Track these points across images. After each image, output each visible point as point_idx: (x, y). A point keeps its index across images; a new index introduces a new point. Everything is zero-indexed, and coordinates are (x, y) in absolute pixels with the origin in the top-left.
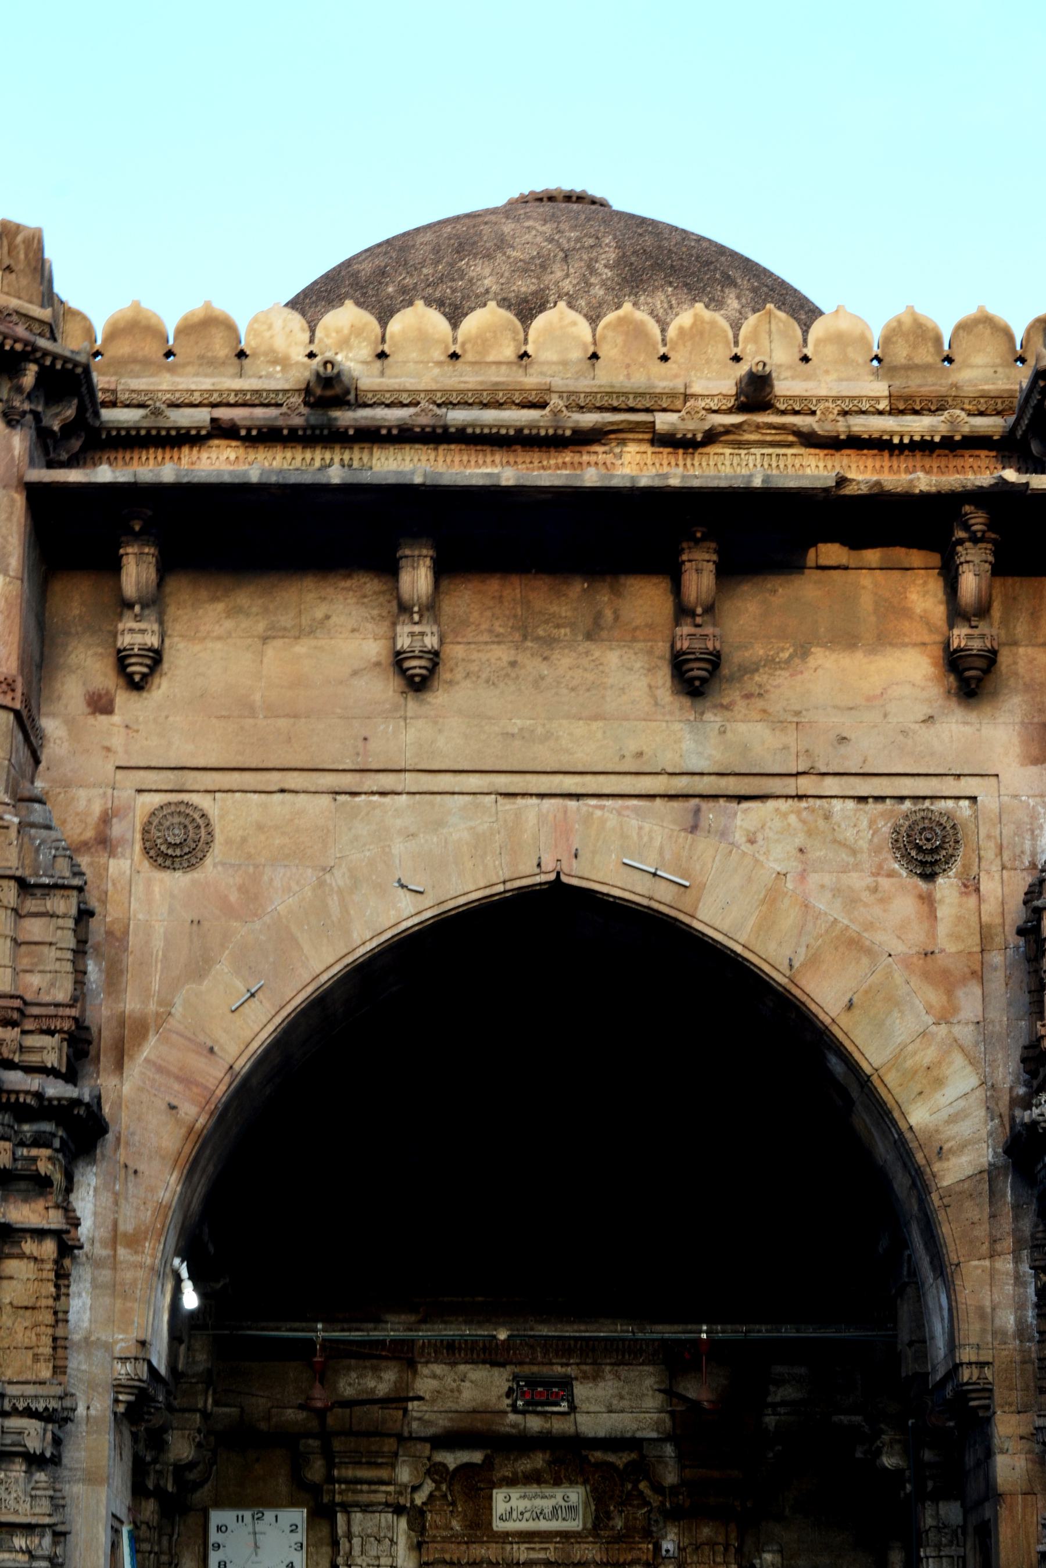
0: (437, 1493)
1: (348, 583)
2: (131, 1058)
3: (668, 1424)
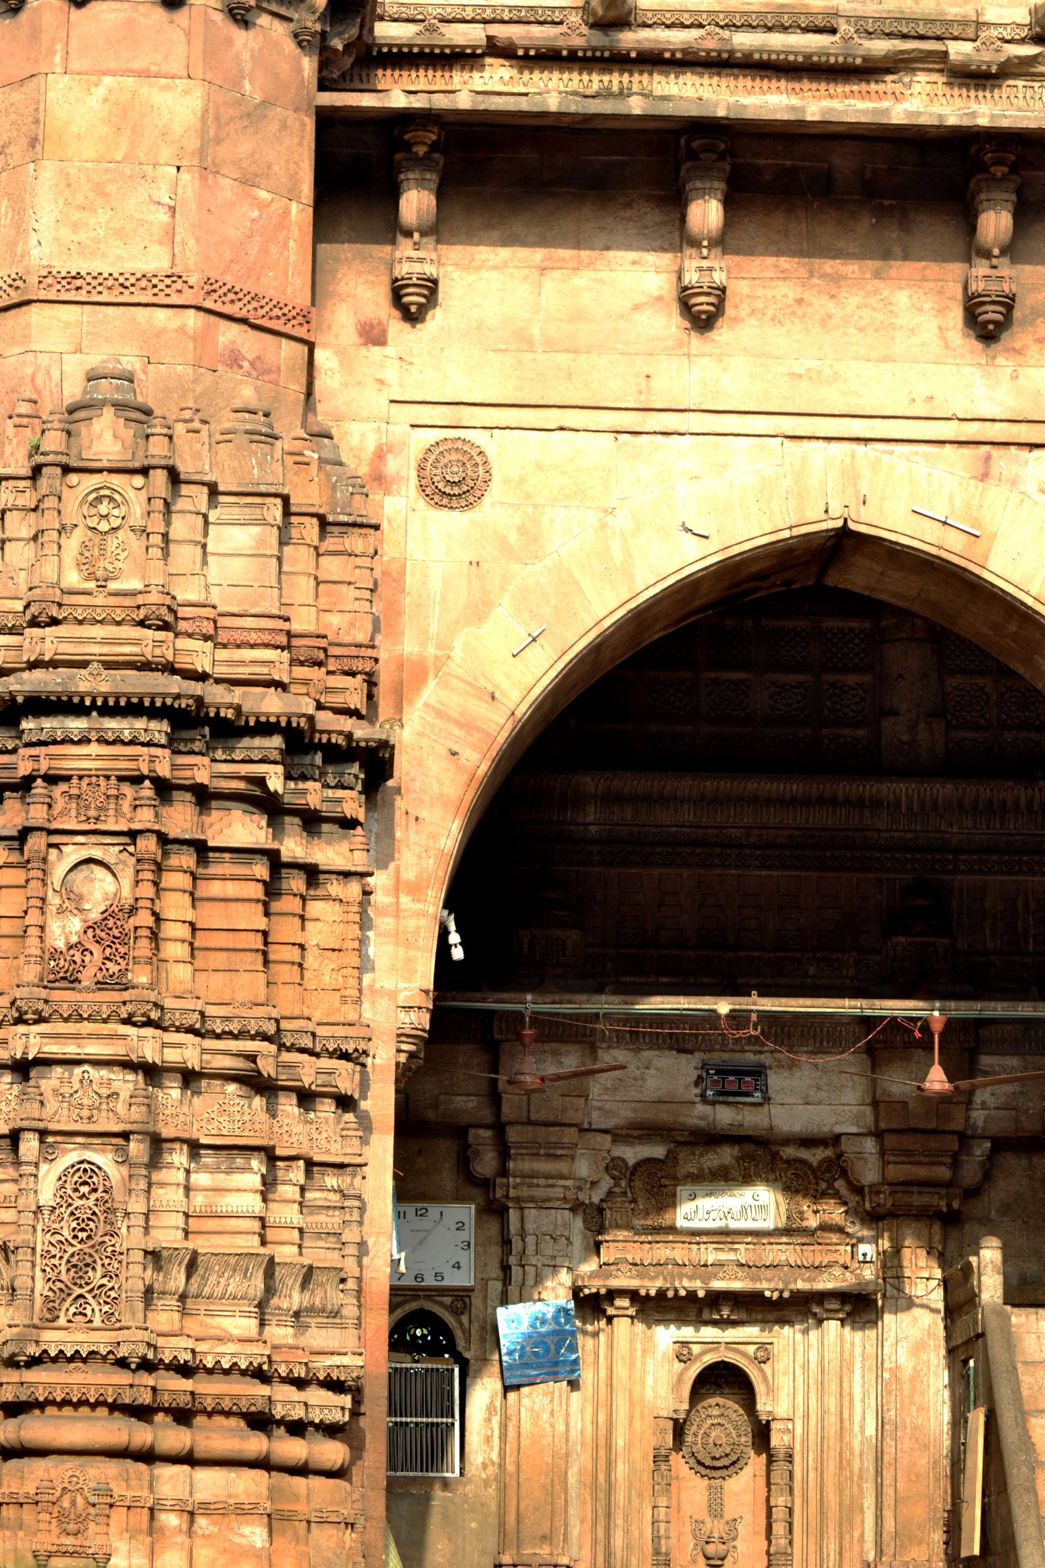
0: (617, 1190)
1: (628, 213)
2: (411, 702)
3: (870, 1118)
